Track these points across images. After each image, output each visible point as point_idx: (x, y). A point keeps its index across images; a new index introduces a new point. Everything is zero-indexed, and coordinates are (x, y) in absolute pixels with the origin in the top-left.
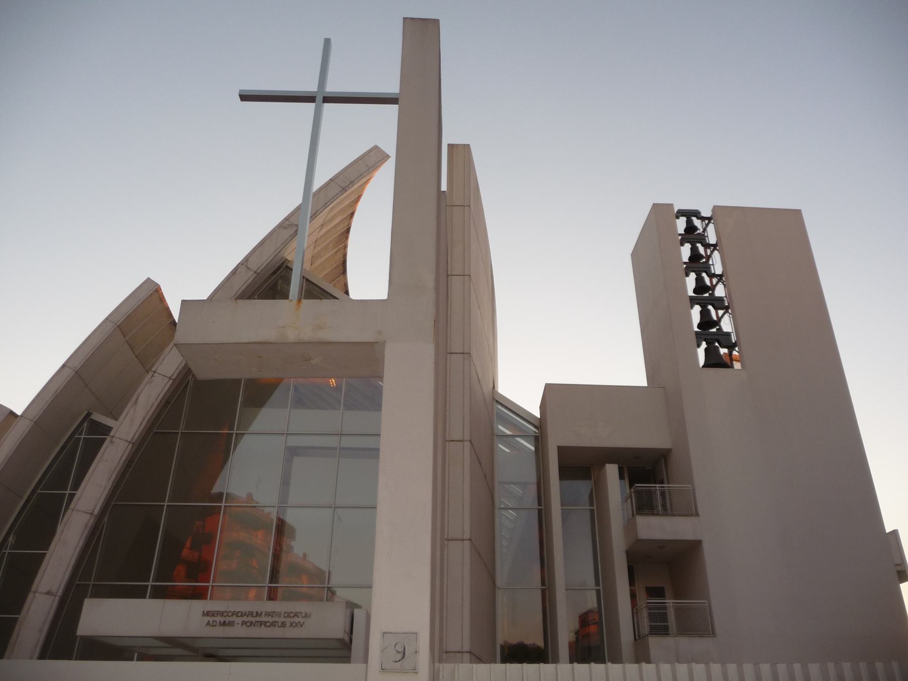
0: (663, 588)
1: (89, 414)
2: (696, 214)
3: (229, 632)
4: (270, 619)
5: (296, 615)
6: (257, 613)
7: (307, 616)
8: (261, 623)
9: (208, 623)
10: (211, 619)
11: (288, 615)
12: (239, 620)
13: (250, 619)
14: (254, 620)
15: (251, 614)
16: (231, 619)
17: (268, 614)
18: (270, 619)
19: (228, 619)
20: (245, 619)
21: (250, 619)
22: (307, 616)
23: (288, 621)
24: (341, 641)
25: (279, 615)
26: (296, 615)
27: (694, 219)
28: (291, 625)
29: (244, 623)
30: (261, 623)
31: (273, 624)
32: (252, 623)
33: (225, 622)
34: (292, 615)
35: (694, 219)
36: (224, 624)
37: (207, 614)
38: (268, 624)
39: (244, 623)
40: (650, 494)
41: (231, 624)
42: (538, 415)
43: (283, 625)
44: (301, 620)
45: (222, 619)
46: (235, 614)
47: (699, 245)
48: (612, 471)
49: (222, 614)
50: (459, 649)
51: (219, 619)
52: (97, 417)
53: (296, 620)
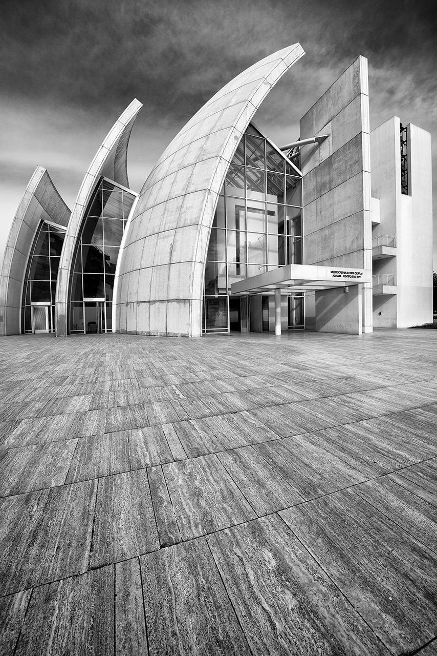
1: (102, 177)
4: (352, 275)
5: (359, 273)
7: (362, 274)
8: (349, 276)
10: (334, 274)
12: (342, 275)
17: (351, 273)
19: (339, 274)
20: (344, 274)
21: (345, 274)
22: (362, 274)
23: (356, 275)
26: (359, 273)
29: (344, 276)
31: (352, 277)
36: (338, 276)
37: (332, 272)
39: (344, 276)
41: (340, 276)
46: (341, 272)
51: (336, 274)
52: (106, 179)
53: (358, 275)
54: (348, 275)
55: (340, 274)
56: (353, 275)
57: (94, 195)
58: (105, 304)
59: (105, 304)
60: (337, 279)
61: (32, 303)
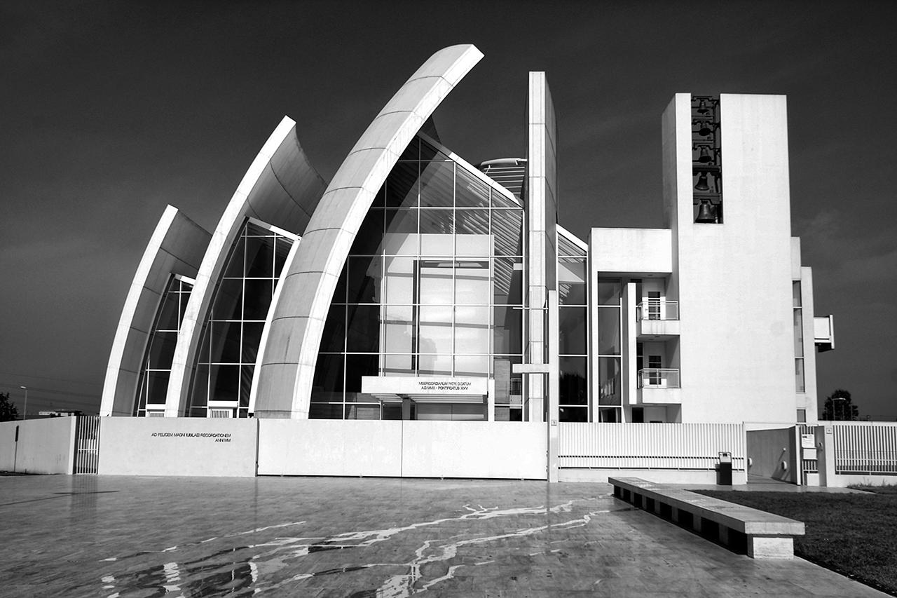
1: (247, 219)
3: (431, 392)
7: (469, 384)
12: (437, 386)
13: (442, 385)
20: (439, 385)
22: (469, 384)
23: (460, 386)
24: (484, 396)
29: (439, 388)
39: (439, 388)
41: (433, 388)
43: (458, 388)
48: (632, 288)
49: (428, 383)
51: (427, 386)
55: (434, 385)
57: (233, 245)
58: (238, 411)
59: (238, 411)
61: (148, 406)
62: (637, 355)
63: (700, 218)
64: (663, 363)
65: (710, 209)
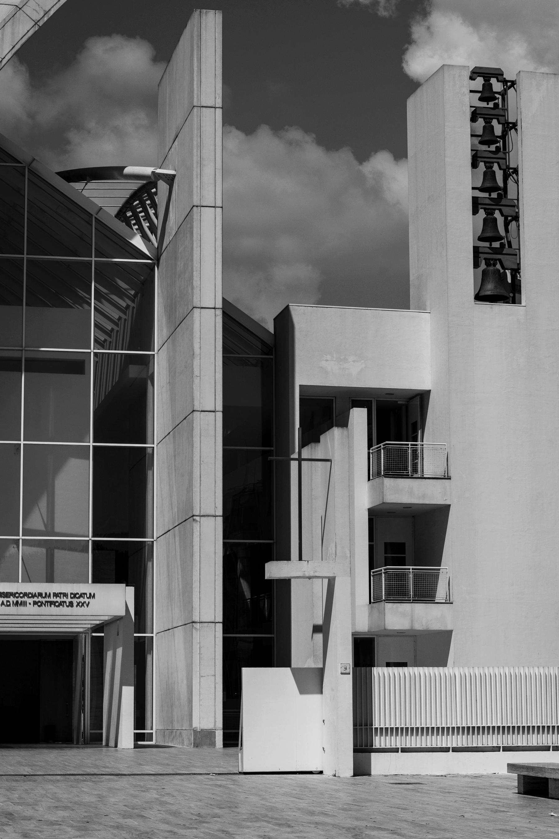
0: (404, 544)
2: (498, 74)
4: (58, 599)
6: (46, 594)
7: (92, 596)
8: (51, 603)
9: (3, 603)
10: (5, 600)
11: (74, 595)
12: (31, 600)
14: (44, 600)
15: (40, 594)
16: (23, 599)
17: (56, 595)
18: (58, 599)
19: (20, 600)
20: (36, 599)
21: (40, 599)
22: (92, 596)
23: (75, 601)
25: (65, 595)
26: (82, 595)
27: (493, 81)
28: (78, 604)
29: (35, 603)
30: (51, 603)
31: (61, 604)
32: (42, 603)
33: (17, 602)
34: (77, 596)
35: (493, 81)
36: (17, 604)
38: (57, 604)
39: (35, 603)
40: (402, 453)
41: (24, 604)
42: (271, 328)
44: (87, 600)
45: (15, 600)
46: (25, 594)
47: (494, 122)
50: (213, 620)
51: (11, 599)
53: (82, 600)
54: (47, 599)
55: (26, 599)
56: (65, 599)
60: (13, 610)
62: (369, 541)
63: (482, 294)
64: (409, 554)
65: (499, 278)
